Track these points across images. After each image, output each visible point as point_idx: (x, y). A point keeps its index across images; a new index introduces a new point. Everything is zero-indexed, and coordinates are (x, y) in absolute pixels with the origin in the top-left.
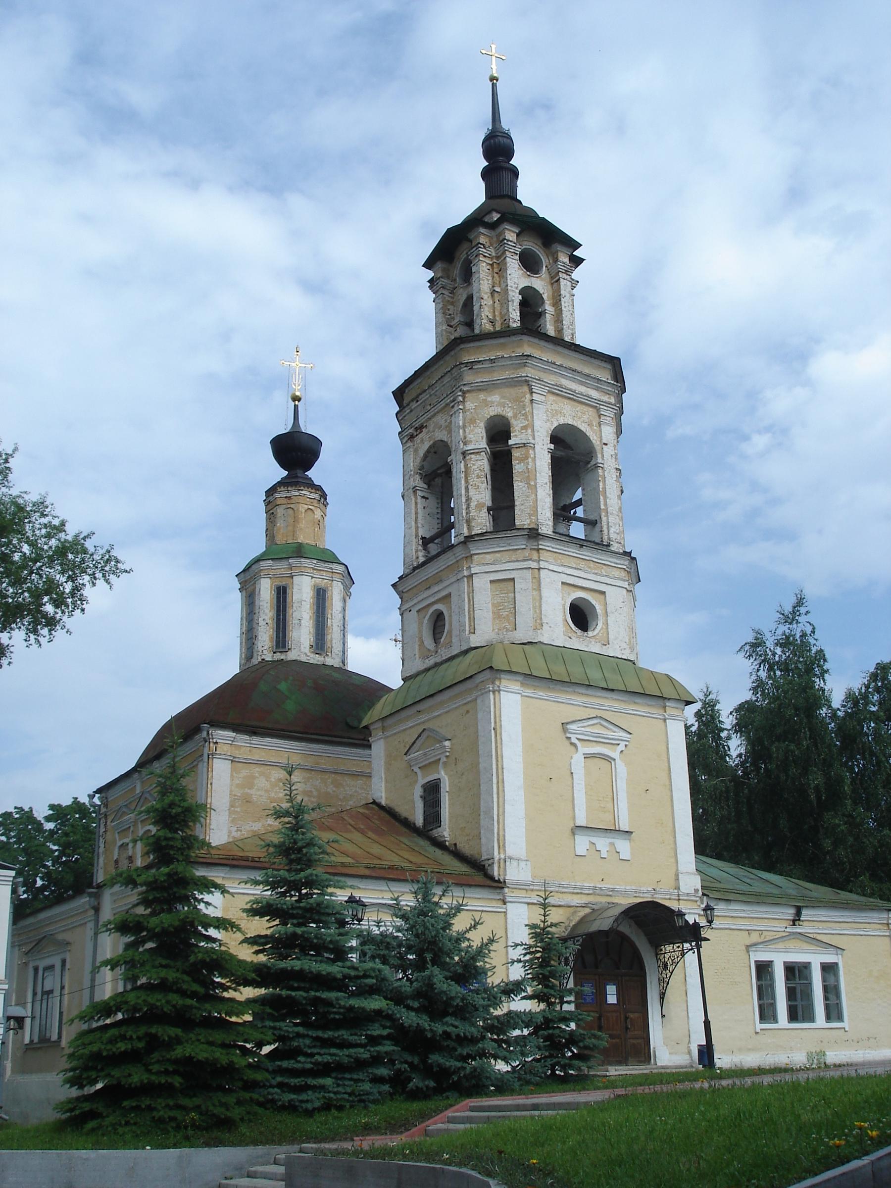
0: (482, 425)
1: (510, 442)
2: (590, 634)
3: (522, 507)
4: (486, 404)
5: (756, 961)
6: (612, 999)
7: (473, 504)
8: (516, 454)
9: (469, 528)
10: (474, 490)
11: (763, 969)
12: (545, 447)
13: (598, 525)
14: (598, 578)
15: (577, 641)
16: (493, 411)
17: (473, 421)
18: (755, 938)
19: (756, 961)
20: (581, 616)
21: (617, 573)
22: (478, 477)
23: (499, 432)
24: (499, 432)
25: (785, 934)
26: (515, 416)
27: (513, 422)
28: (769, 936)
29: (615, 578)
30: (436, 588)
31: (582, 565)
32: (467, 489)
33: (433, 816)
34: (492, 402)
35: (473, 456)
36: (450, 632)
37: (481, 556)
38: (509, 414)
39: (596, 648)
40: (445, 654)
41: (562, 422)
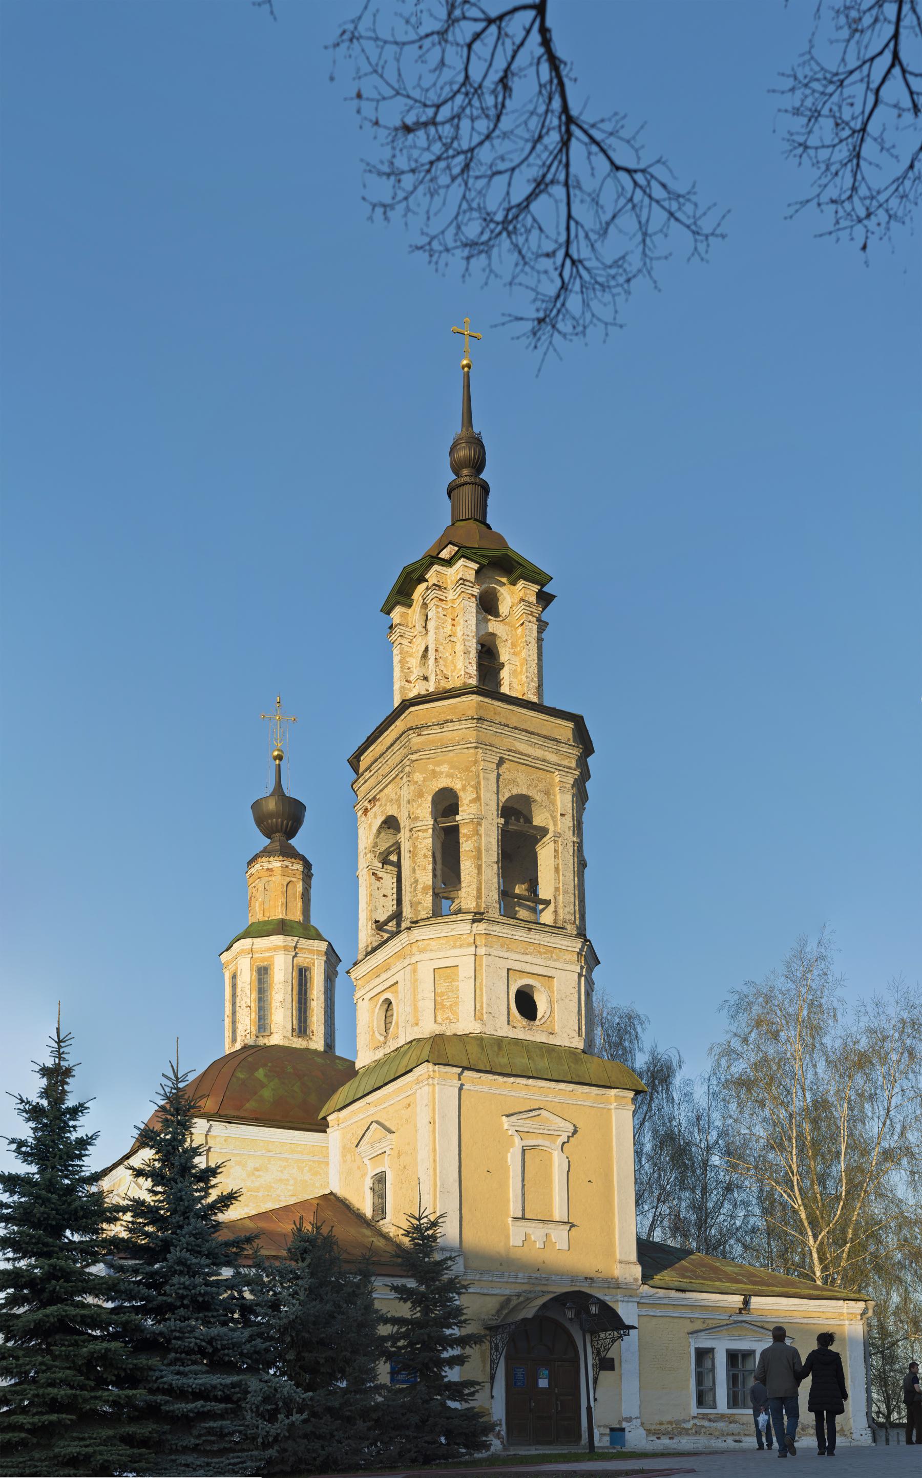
0: (430, 799)
1: (458, 818)
2: (537, 1022)
3: (468, 890)
4: (435, 774)
5: (696, 1349)
6: (543, 1383)
7: (420, 887)
8: (463, 831)
9: (416, 912)
10: (420, 872)
11: (703, 1355)
12: (495, 822)
13: (552, 905)
14: (548, 963)
15: (520, 1030)
16: (443, 783)
17: (420, 795)
18: (698, 1325)
19: (696, 1349)
20: (526, 1004)
21: (568, 957)
22: (425, 856)
23: (446, 804)
24: (446, 804)
25: (728, 1322)
26: (464, 788)
27: (461, 794)
28: (712, 1323)
29: (565, 961)
30: (384, 976)
31: (531, 949)
32: (414, 870)
33: (380, 1210)
34: (442, 773)
35: (420, 834)
36: (397, 1024)
37: (426, 942)
38: (457, 786)
39: (541, 1037)
40: (392, 1045)
41: (514, 792)
